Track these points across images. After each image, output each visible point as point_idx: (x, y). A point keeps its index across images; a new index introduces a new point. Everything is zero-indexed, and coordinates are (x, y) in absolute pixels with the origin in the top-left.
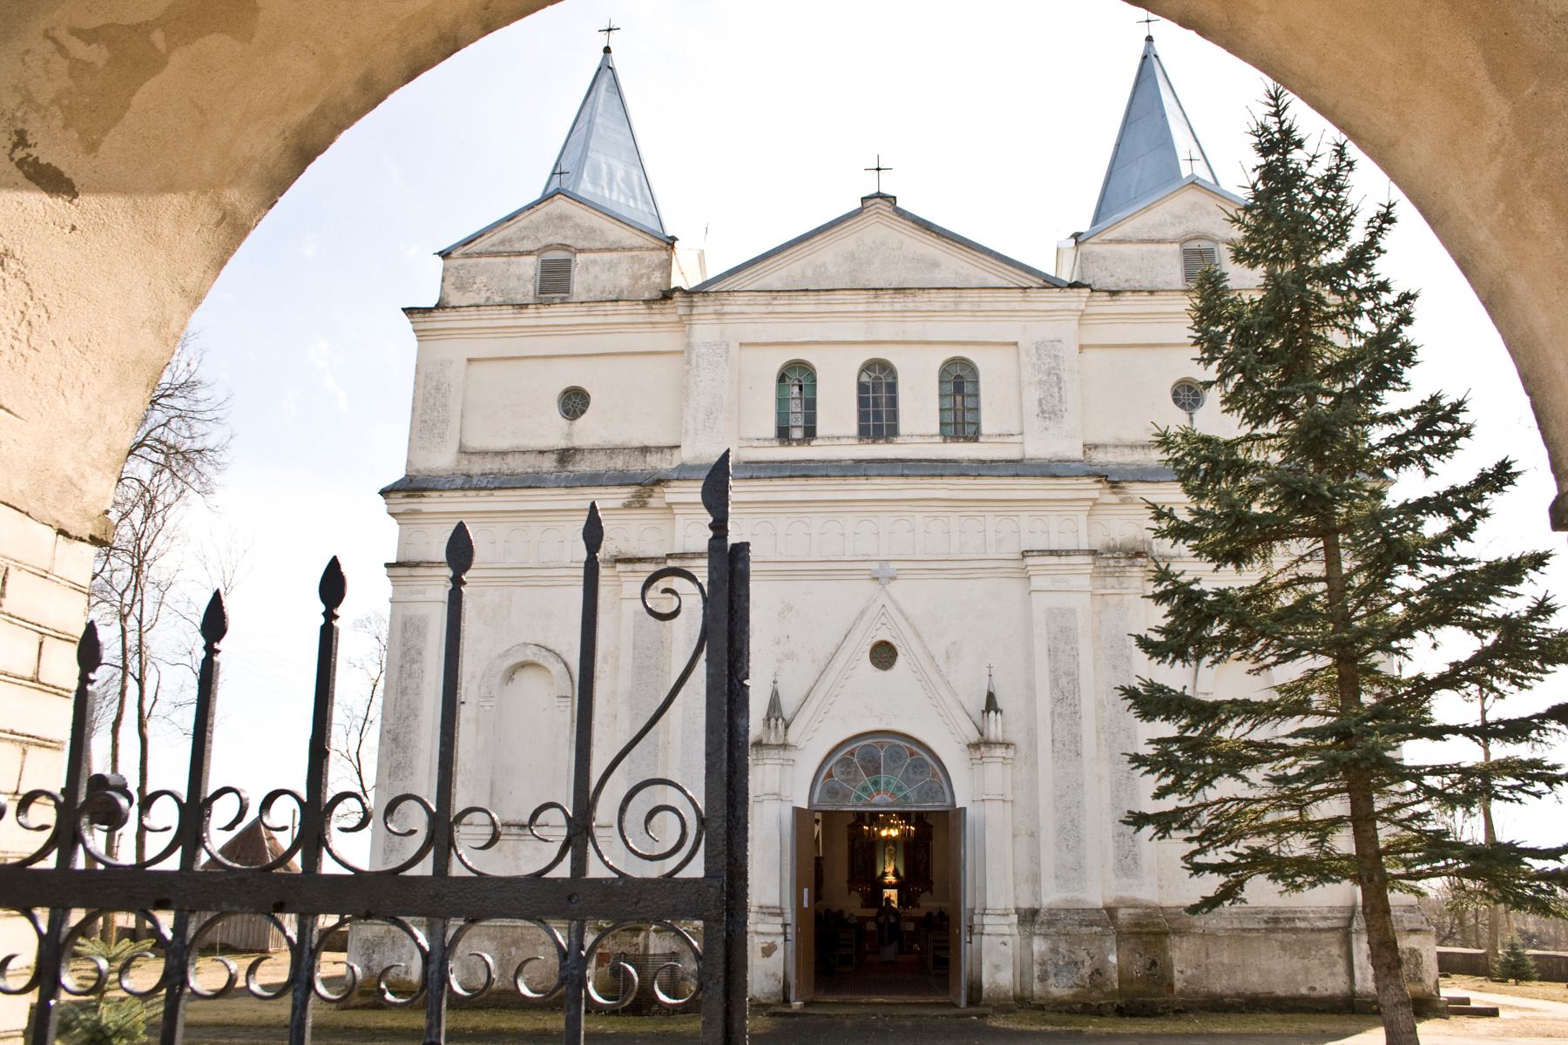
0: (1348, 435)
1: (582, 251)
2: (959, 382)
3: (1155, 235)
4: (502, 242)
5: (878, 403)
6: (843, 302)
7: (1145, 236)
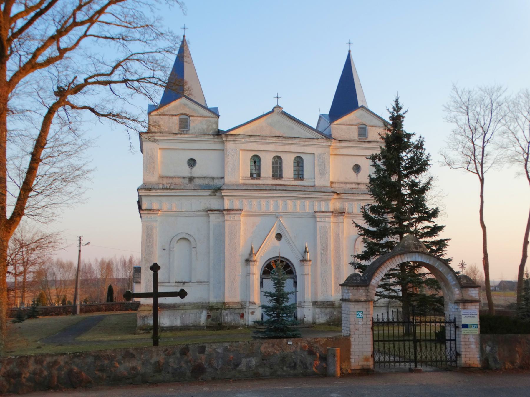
0: (391, 313)
1: (192, 116)
2: (299, 162)
3: (351, 123)
4: (167, 111)
5: (277, 172)
6: (268, 140)
7: (348, 123)
